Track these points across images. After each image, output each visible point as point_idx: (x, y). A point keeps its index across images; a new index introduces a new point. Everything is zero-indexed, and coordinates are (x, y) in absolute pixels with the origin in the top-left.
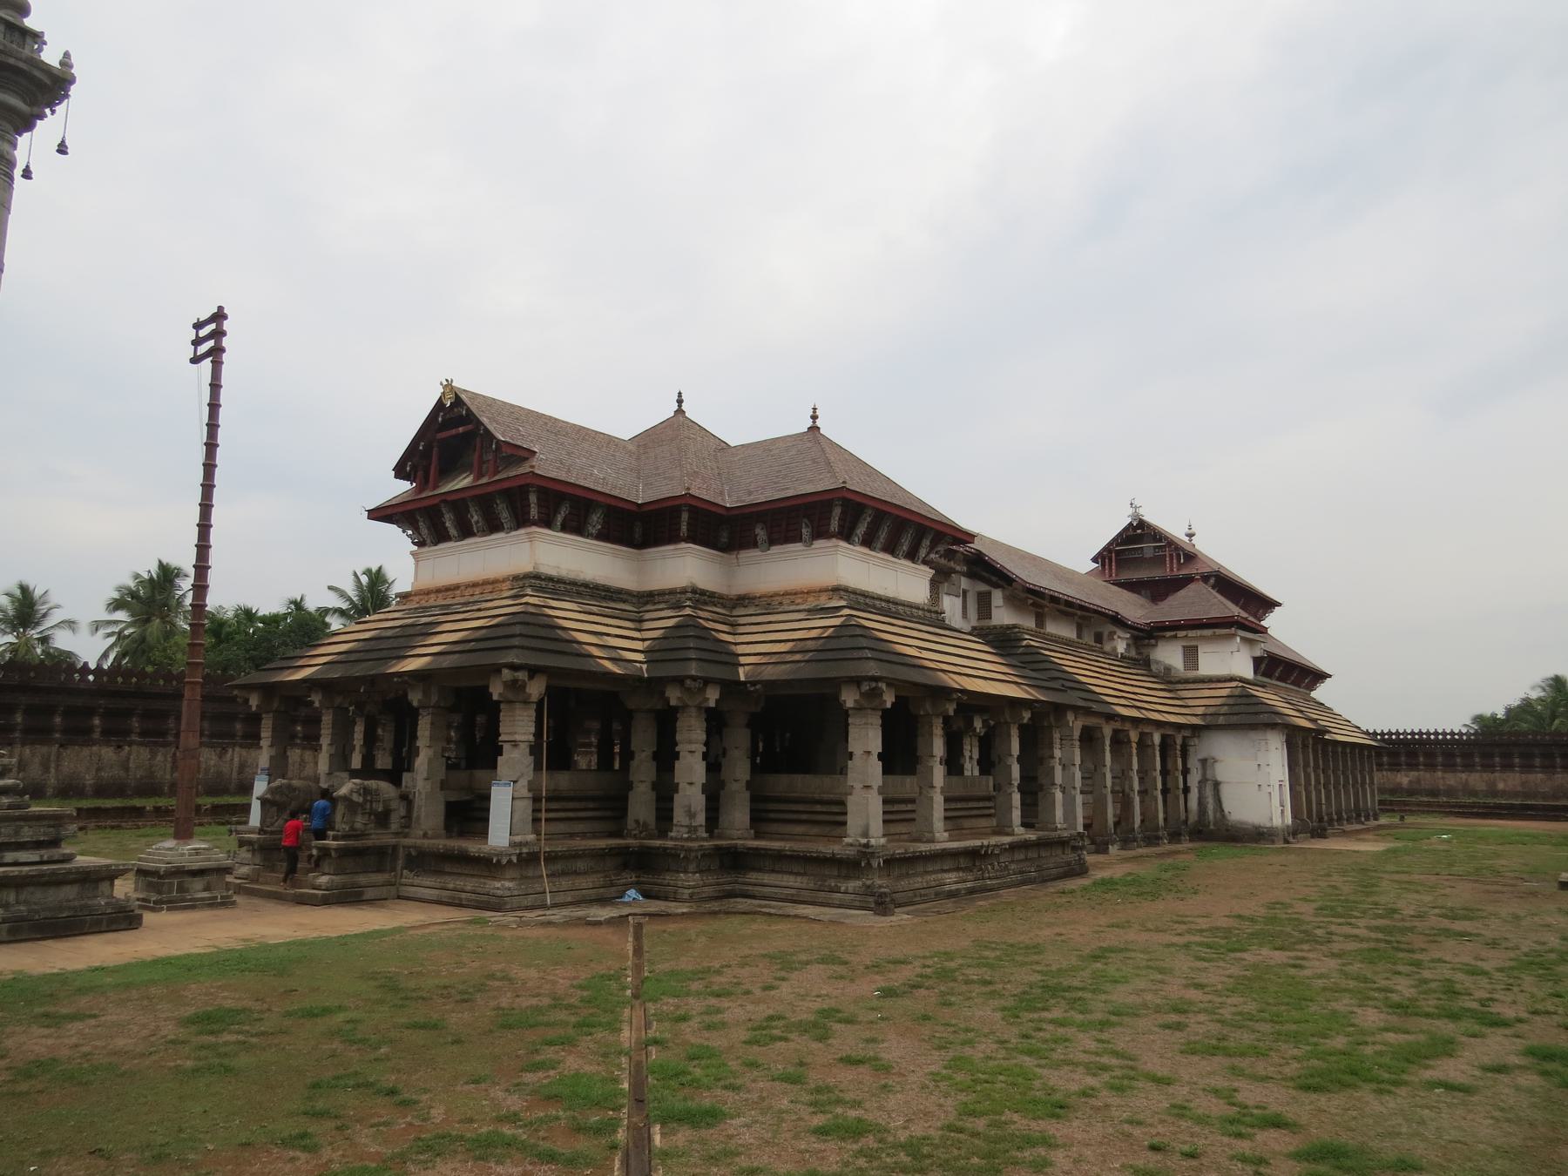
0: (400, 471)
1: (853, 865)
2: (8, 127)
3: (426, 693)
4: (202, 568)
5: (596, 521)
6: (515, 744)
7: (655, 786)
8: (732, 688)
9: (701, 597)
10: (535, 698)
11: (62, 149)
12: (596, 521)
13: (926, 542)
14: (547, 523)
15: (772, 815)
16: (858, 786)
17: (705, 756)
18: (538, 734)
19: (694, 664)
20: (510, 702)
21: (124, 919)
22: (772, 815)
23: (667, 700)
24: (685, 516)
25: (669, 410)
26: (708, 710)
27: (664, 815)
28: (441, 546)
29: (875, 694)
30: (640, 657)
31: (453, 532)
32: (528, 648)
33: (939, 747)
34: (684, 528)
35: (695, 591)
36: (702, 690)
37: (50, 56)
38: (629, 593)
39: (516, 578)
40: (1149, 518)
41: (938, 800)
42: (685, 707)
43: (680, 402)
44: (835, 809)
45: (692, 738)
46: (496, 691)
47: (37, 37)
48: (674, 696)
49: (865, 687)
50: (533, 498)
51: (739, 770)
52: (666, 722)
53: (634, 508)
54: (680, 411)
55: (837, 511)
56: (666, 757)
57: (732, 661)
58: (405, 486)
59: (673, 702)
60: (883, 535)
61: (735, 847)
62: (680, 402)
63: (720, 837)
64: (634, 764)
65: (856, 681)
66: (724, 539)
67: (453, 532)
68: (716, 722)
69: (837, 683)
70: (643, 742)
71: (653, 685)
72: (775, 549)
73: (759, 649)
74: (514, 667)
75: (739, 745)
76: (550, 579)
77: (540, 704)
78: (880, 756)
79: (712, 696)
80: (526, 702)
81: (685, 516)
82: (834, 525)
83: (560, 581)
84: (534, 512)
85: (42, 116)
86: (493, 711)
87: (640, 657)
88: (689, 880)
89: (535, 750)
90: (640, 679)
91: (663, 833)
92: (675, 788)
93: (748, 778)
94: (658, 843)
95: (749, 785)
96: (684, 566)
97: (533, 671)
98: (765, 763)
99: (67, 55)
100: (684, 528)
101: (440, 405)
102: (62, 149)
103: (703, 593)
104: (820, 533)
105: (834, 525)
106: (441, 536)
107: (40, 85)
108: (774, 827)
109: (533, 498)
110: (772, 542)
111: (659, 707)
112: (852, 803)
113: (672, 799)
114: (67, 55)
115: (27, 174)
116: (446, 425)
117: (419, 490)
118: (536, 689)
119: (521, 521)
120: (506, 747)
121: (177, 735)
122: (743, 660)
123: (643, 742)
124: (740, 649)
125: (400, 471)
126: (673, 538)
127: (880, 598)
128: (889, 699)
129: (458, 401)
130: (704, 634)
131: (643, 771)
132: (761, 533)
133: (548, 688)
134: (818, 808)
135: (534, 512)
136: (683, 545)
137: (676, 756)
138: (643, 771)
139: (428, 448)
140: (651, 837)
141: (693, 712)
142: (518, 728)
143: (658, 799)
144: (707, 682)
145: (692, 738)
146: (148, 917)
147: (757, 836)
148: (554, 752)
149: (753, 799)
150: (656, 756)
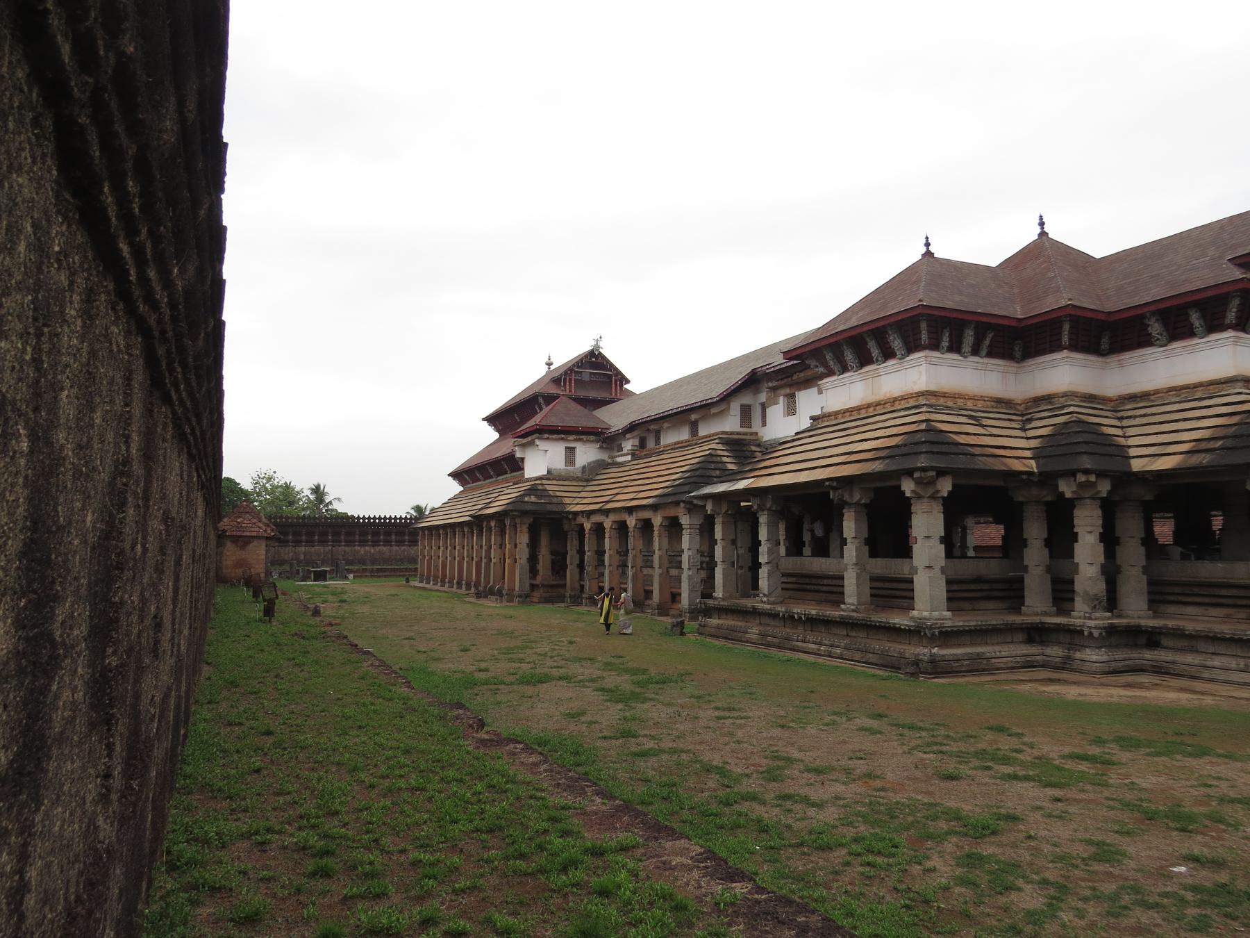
7: (1049, 569)
8: (1125, 479)
14: (935, 346)
15: (1172, 598)
19: (1085, 458)
20: (919, 497)
22: (1172, 598)
23: (1062, 494)
24: (1066, 327)
27: (1062, 592)
28: (846, 375)
30: (1028, 454)
32: (932, 453)
34: (1065, 338)
40: (609, 352)
43: (1042, 224)
45: (1087, 524)
46: (908, 487)
48: (1067, 489)
50: (923, 325)
51: (1132, 554)
53: (1014, 324)
54: (1043, 234)
56: (1061, 539)
57: (1122, 453)
59: (1068, 495)
61: (1139, 626)
62: (1042, 224)
63: (1120, 616)
64: (1026, 552)
66: (1105, 346)
68: (1109, 509)
70: (1035, 531)
71: (1046, 479)
79: (1104, 488)
80: (933, 497)
81: (1066, 327)
82: (1231, 316)
84: (924, 337)
87: (1028, 454)
88: (1094, 656)
90: (1032, 473)
93: (1144, 563)
94: (1058, 620)
95: (1145, 570)
96: (1063, 373)
97: (941, 473)
100: (1065, 338)
105: (1231, 316)
108: (1172, 609)
109: (923, 325)
111: (1049, 498)
113: (1072, 582)
118: (945, 487)
119: (912, 347)
123: (1035, 531)
124: (1131, 442)
126: (1056, 347)
130: (1092, 430)
131: (1035, 555)
133: (954, 486)
134: (1224, 592)
135: (924, 337)
136: (1065, 353)
138: (1035, 555)
143: (1055, 581)
145: (1087, 524)
147: (1157, 614)
149: (1151, 583)
150: (1048, 543)
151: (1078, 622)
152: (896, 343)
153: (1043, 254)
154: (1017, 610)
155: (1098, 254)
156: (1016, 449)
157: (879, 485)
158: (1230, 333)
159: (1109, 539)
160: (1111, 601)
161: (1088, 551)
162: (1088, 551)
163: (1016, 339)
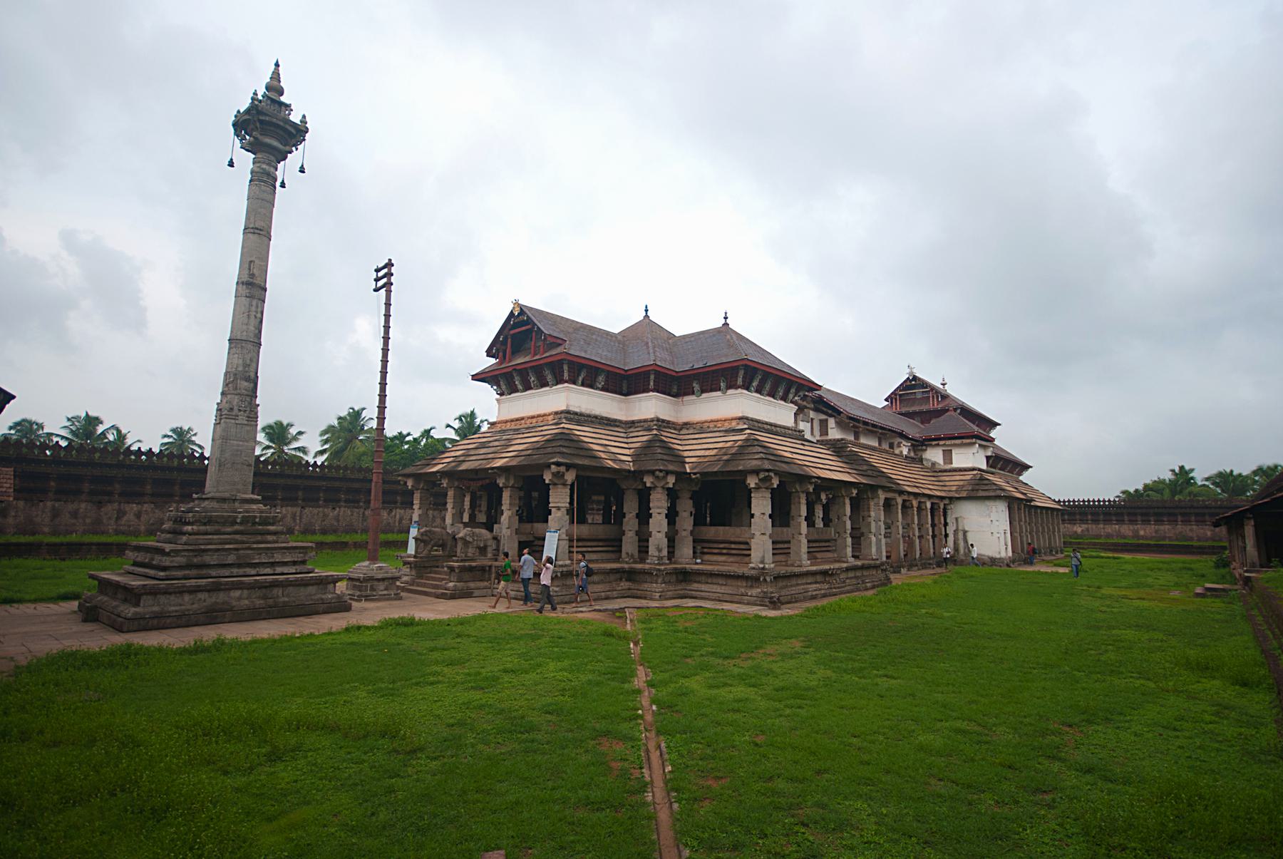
0: (489, 353)
1: (754, 580)
2: (272, 158)
3: (507, 479)
4: (382, 408)
5: (601, 380)
6: (559, 508)
7: (637, 533)
8: (682, 476)
9: (662, 424)
10: (569, 482)
11: (302, 170)
12: (601, 380)
13: (793, 390)
16: (757, 534)
17: (667, 516)
18: (571, 503)
20: (555, 484)
21: (342, 606)
24: (652, 377)
25: (719, 323)
26: (668, 489)
27: (643, 550)
29: (767, 479)
30: (629, 459)
31: (520, 387)
33: (804, 512)
35: (658, 420)
36: (665, 477)
37: (295, 118)
38: (620, 421)
39: (556, 413)
41: (804, 541)
42: (655, 487)
44: (742, 547)
45: (659, 504)
47: (288, 106)
49: (762, 475)
50: (566, 367)
51: (686, 522)
52: (644, 497)
55: (741, 373)
56: (644, 516)
58: (493, 361)
60: (768, 387)
65: (756, 472)
67: (520, 387)
68: (672, 494)
69: (745, 473)
71: (637, 475)
72: (704, 395)
73: (696, 453)
74: (558, 464)
75: (686, 509)
76: (576, 413)
77: (572, 485)
78: (770, 516)
79: (671, 480)
80: (564, 485)
81: (652, 377)
82: (740, 381)
83: (581, 415)
84: (566, 376)
85: (291, 152)
86: (545, 490)
87: (629, 459)
88: (657, 587)
89: (570, 511)
90: (629, 471)
91: (642, 560)
92: (650, 535)
94: (639, 566)
95: (692, 533)
97: (569, 467)
98: (699, 521)
99: (304, 117)
101: (512, 313)
102: (302, 170)
103: (663, 421)
104: (732, 385)
105: (740, 381)
106: (513, 390)
107: (290, 133)
109: (566, 367)
110: (703, 391)
112: (753, 543)
114: (304, 117)
115: (283, 185)
116: (516, 325)
117: (500, 363)
118: (570, 477)
119: (559, 381)
120: (553, 510)
121: (369, 502)
122: (687, 460)
123: (631, 507)
124: (686, 454)
125: (489, 353)
126: (646, 390)
127: (767, 423)
128: (775, 482)
129: (522, 312)
132: (696, 386)
135: (566, 376)
137: (650, 516)
138: (630, 523)
139: (506, 338)
140: (635, 562)
141: (659, 490)
142: (559, 499)
144: (668, 473)
145: (659, 504)
146: (354, 604)
148: (578, 514)
151: (647, 567)
152: (549, 378)
153: (647, 329)
154: (618, 560)
155: (678, 332)
156: (617, 452)
157: (529, 474)
158: (740, 390)
159: (672, 516)
160: (671, 554)
161: (658, 523)
162: (658, 523)
163: (625, 383)
